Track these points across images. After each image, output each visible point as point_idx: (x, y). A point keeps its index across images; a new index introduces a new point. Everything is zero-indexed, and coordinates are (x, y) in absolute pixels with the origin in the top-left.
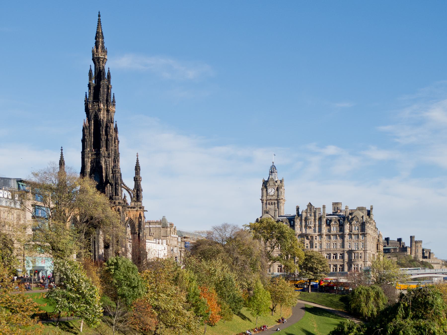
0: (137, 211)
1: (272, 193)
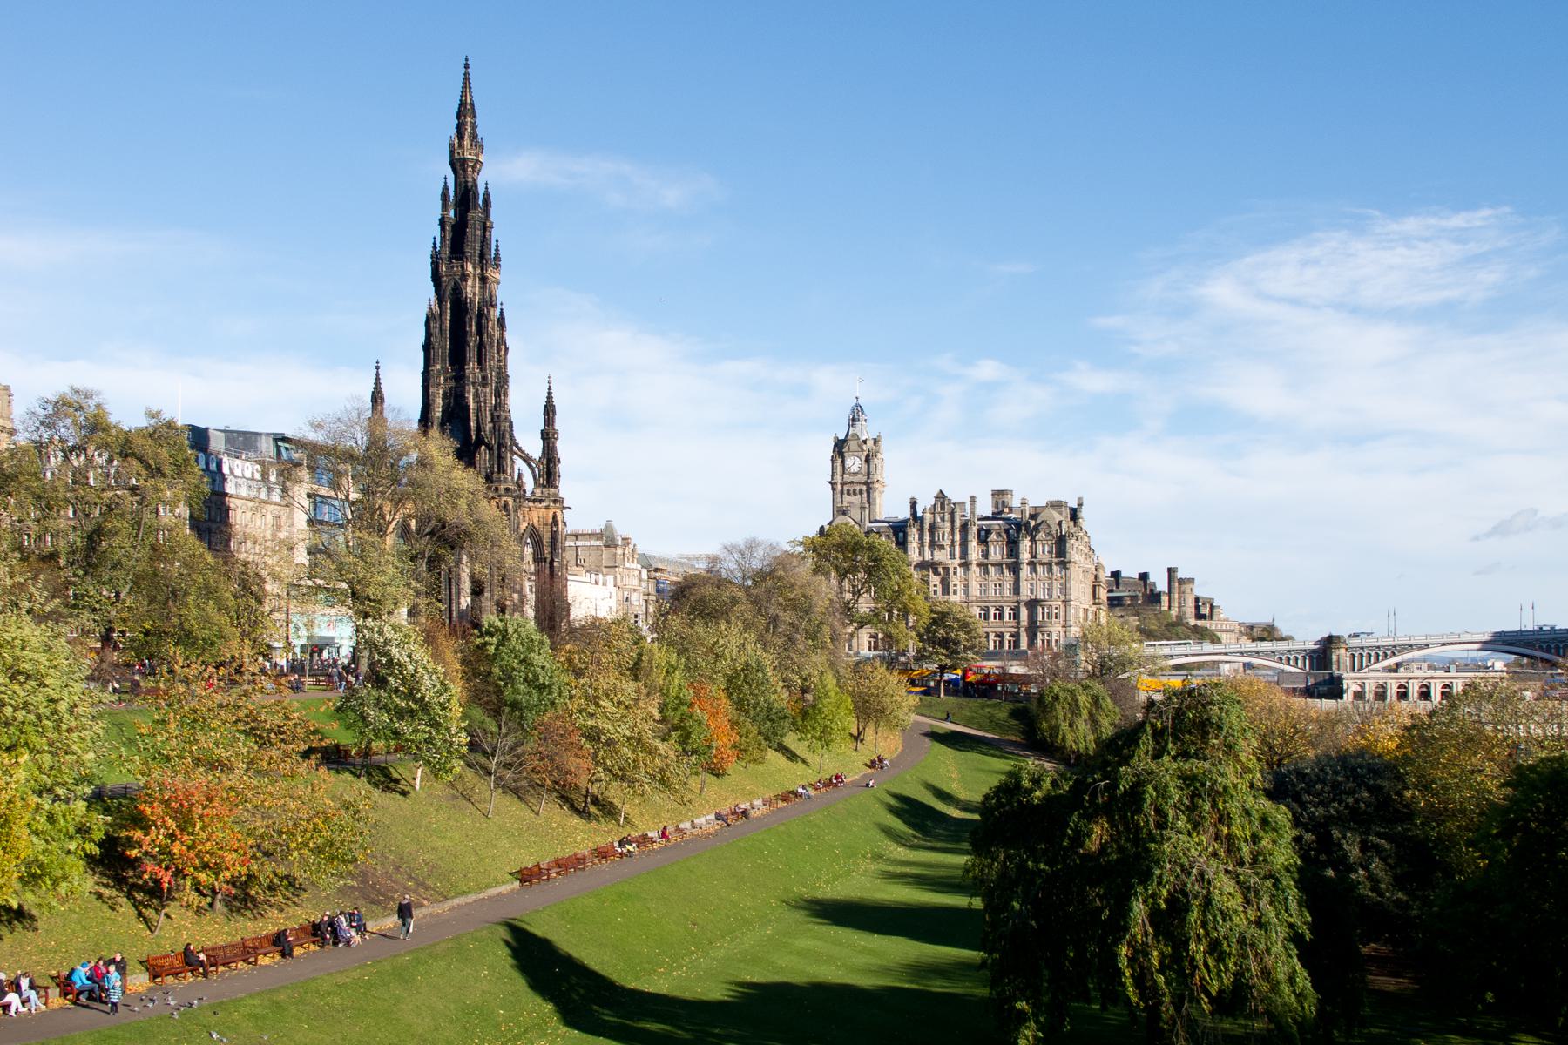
0: (547, 508)
1: (855, 469)
